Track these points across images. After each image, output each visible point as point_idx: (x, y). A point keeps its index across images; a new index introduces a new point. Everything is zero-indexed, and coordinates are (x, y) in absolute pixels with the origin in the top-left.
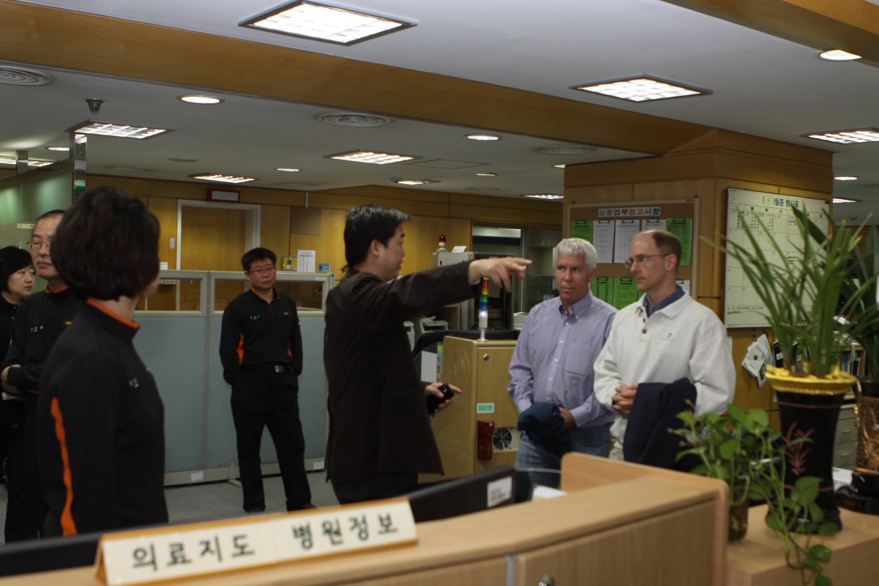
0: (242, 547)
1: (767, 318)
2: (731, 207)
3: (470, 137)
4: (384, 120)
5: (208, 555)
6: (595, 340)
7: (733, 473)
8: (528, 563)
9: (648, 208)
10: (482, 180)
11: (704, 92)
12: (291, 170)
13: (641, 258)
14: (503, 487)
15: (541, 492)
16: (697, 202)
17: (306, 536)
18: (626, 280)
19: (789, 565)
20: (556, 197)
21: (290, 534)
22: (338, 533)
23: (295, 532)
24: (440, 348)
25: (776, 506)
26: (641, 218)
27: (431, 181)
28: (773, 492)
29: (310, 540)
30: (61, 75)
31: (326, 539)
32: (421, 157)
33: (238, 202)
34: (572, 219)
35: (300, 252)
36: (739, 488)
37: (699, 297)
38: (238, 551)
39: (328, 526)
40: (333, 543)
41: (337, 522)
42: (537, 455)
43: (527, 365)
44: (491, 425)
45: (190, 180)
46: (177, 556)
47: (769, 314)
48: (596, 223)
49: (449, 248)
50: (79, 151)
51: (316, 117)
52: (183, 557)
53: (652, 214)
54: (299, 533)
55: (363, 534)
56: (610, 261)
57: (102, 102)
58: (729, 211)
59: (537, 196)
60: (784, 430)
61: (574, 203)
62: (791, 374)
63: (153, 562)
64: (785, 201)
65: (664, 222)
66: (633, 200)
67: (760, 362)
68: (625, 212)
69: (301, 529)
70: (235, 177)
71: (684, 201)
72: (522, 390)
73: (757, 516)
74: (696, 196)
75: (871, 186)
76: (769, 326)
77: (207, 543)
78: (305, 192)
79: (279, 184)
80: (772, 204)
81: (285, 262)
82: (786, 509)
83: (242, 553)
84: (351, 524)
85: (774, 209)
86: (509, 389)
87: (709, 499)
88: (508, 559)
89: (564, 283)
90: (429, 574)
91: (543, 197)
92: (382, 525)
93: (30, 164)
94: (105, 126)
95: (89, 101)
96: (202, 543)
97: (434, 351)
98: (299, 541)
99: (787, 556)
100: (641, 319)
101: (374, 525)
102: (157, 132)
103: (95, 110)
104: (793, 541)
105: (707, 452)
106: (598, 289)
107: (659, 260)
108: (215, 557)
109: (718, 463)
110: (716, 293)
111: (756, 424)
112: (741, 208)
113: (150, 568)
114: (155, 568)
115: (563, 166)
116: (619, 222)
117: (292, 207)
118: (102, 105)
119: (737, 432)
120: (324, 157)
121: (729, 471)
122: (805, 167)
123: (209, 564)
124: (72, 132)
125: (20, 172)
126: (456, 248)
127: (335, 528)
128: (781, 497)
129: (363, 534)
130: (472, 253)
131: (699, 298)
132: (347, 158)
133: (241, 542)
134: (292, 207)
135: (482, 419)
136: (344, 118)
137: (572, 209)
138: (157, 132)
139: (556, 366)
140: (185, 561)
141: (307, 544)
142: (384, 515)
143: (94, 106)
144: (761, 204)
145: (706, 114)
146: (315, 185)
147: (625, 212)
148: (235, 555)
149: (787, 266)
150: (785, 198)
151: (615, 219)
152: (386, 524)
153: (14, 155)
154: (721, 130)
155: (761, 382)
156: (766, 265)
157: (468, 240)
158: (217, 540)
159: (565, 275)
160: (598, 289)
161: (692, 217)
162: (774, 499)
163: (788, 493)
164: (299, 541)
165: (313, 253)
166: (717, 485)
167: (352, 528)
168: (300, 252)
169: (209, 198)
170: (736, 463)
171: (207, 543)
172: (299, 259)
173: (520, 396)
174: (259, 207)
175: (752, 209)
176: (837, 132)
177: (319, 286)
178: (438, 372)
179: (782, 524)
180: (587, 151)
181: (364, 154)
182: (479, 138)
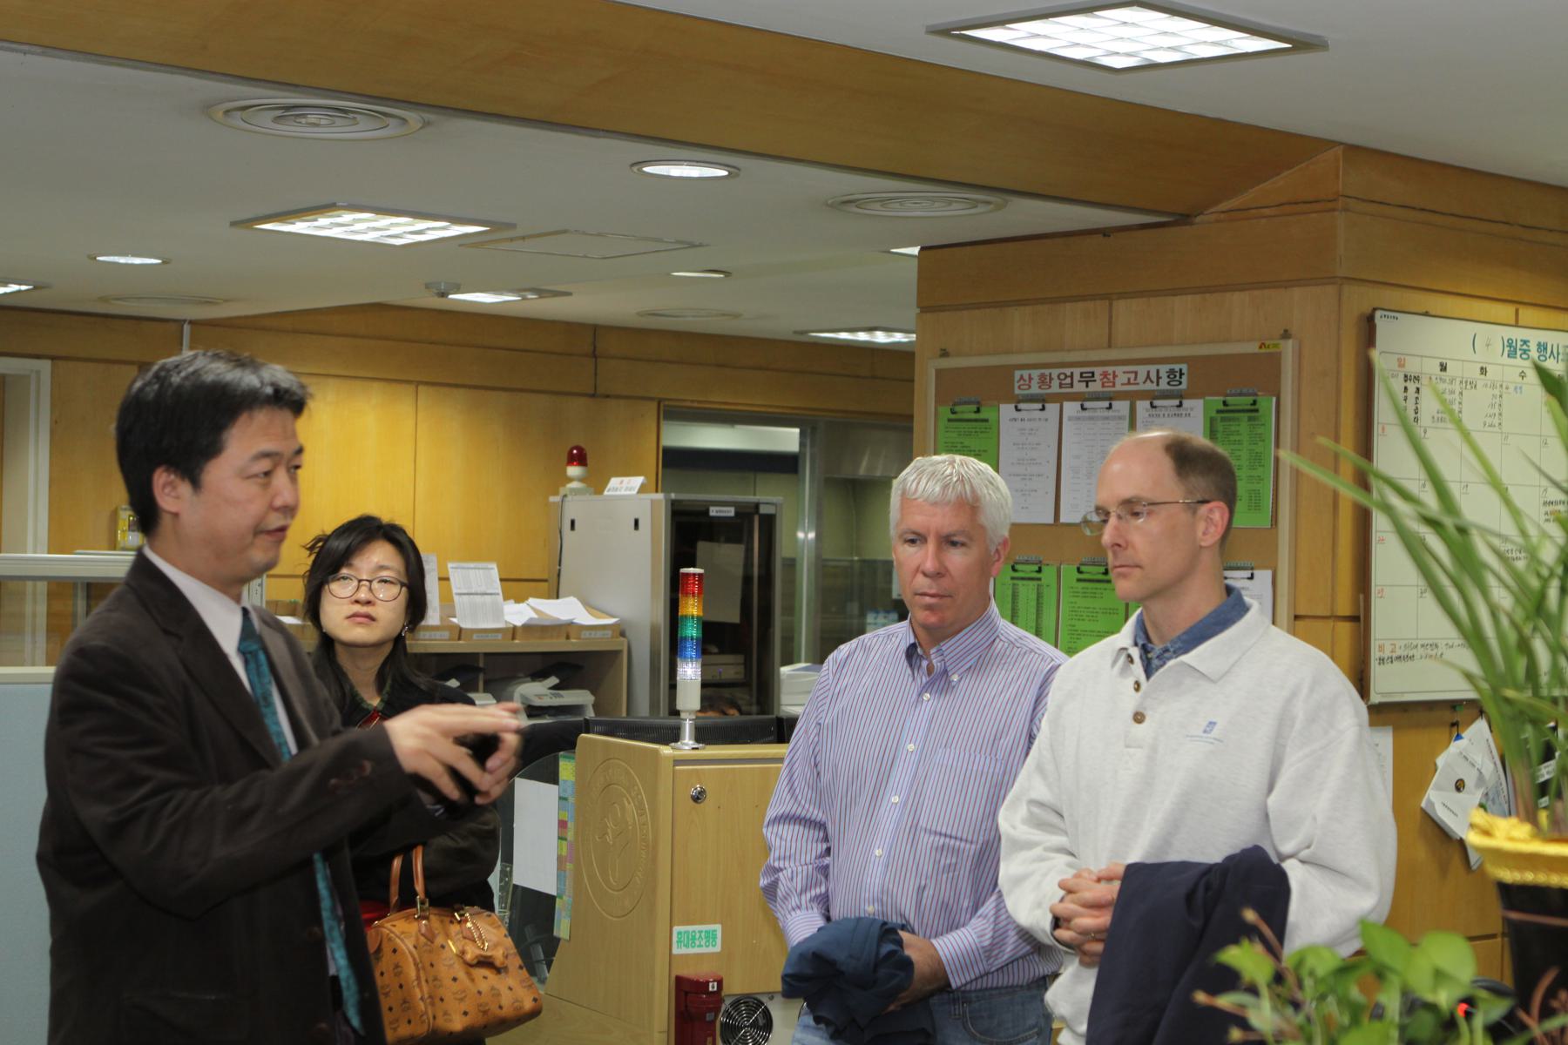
3: (647, 169)
4: (404, 121)
6: (1005, 742)
9: (1153, 369)
10: (685, 293)
11: (1301, 44)
12: (138, 261)
13: (1132, 507)
16: (1288, 348)
18: (1094, 571)
20: (898, 337)
26: (1133, 397)
27: (541, 293)
32: (512, 226)
34: (938, 402)
37: (1297, 617)
43: (817, 815)
44: (713, 987)
48: (1007, 410)
49: (596, 484)
51: (207, 108)
53: (1164, 385)
56: (1051, 521)
59: (844, 336)
61: (945, 354)
65: (1196, 406)
66: (1110, 346)
68: (1088, 379)
71: (1252, 348)
72: (799, 883)
74: (1286, 335)
78: (180, 323)
86: (763, 882)
89: (922, 582)
91: (862, 336)
97: (552, 778)
100: (1130, 682)
106: (1015, 596)
107: (1184, 517)
110: (1344, 608)
112: (1412, 367)
115: (915, 251)
116: (1071, 408)
120: (233, 224)
130: (660, 496)
131: (1298, 622)
132: (300, 227)
135: (689, 972)
136: (288, 112)
137: (940, 373)
146: (209, 302)
147: (1088, 379)
150: (1534, 337)
151: (1060, 398)
154: (1353, 151)
157: (651, 459)
160: (1015, 596)
173: (794, 901)
174: (45, 365)
175: (1443, 368)
180: (981, 209)
181: (347, 217)
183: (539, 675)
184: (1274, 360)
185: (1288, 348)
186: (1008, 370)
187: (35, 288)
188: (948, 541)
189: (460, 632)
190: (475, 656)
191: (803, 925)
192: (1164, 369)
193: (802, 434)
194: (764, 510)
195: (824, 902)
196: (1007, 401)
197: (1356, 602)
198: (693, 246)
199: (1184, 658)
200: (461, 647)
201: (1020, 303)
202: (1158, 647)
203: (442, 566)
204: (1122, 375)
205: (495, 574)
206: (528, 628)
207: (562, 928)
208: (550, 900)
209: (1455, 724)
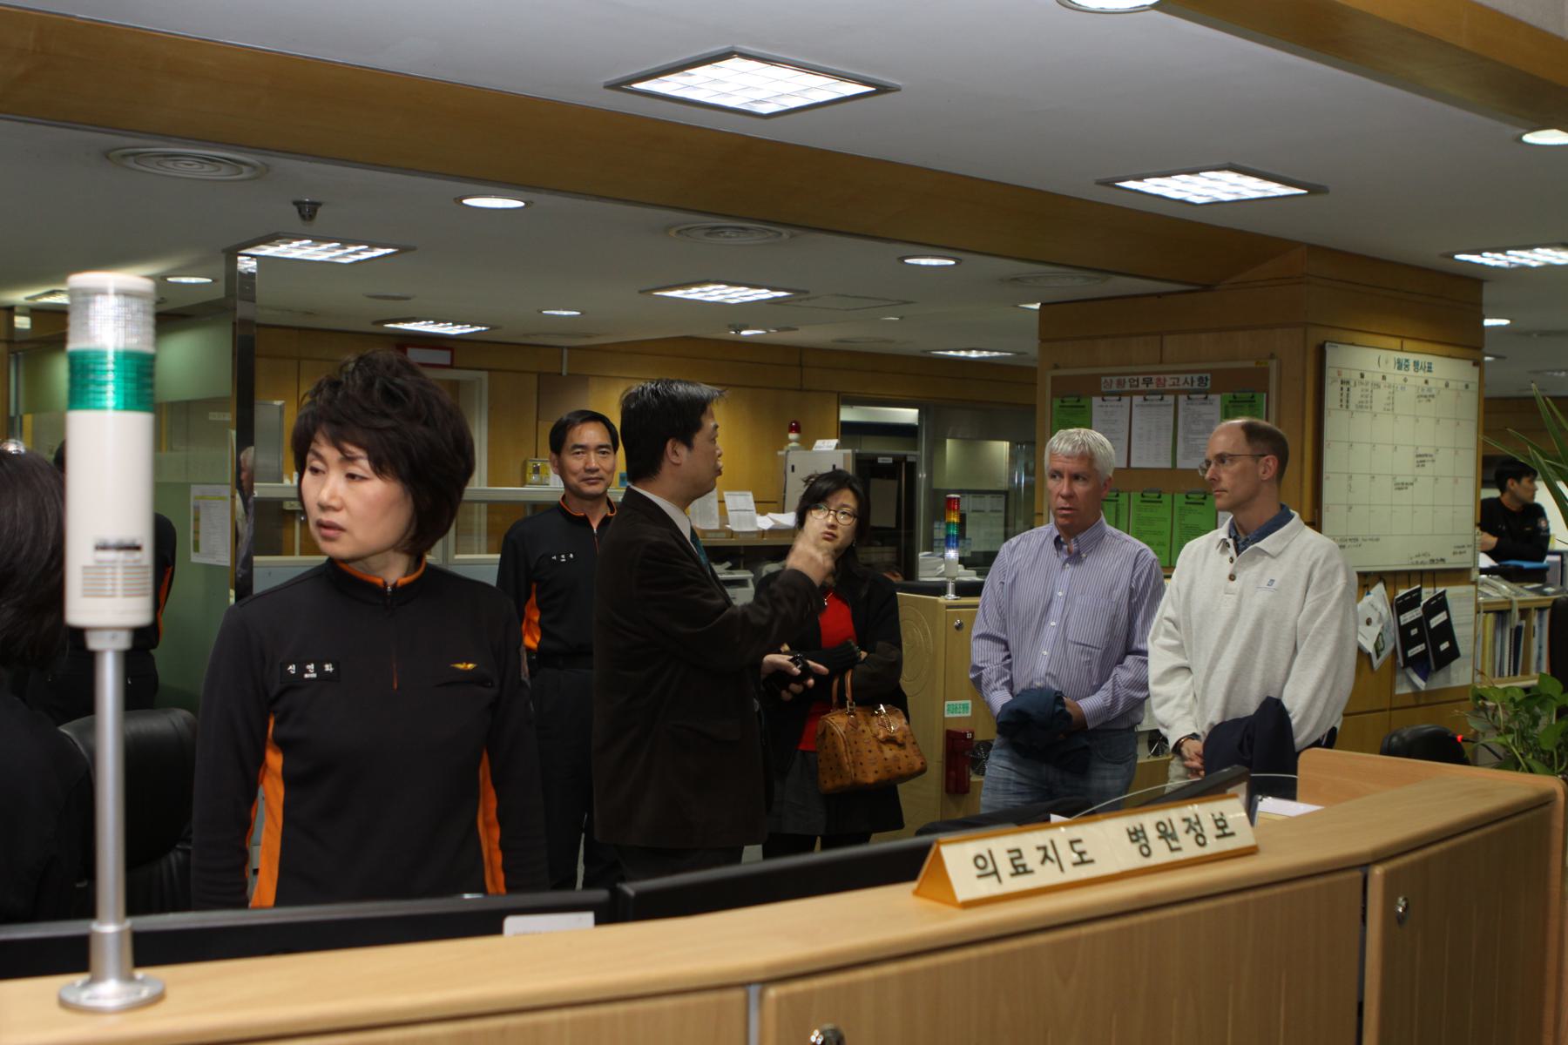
0: (1081, 854)
2: (1330, 373)
5: (1048, 863)
6: (1117, 593)
10: (885, 330)
11: (1314, 190)
13: (1221, 458)
16: (1273, 364)
20: (985, 354)
21: (1126, 836)
22: (1175, 839)
23: (1130, 834)
26: (1176, 393)
31: (1163, 842)
32: (806, 292)
33: (451, 366)
34: (1054, 395)
40: (1172, 850)
42: (1023, 780)
43: (1003, 636)
44: (969, 736)
48: (1096, 401)
49: (807, 444)
52: (1024, 866)
53: (1196, 386)
55: (1200, 839)
56: (1124, 465)
57: (318, 204)
58: (1328, 381)
59: (952, 353)
61: (1056, 367)
63: (996, 872)
65: (1216, 399)
66: (1161, 362)
67: (1375, 630)
68: (1148, 382)
69: (1136, 832)
71: (1252, 364)
72: (994, 676)
74: (1272, 356)
75: (1528, 334)
77: (1045, 848)
78: (561, 348)
79: (526, 335)
80: (1391, 369)
81: (530, 470)
83: (1083, 862)
84: (1186, 825)
85: (1396, 377)
86: (972, 676)
89: (1061, 502)
90: (1322, 881)
91: (962, 354)
94: (296, 244)
95: (299, 204)
98: (1136, 846)
100: (1227, 557)
101: (1210, 829)
103: (308, 218)
108: (1056, 865)
112: (1345, 376)
113: (994, 878)
114: (1000, 880)
115: (1037, 306)
116: (1137, 399)
117: (539, 374)
118: (320, 211)
122: (1440, 305)
123: (1046, 875)
124: (232, 254)
126: (819, 443)
127: (1170, 830)
129: (1200, 839)
130: (849, 451)
132: (678, 293)
134: (539, 374)
135: (953, 727)
136: (713, 231)
137: (1054, 379)
139: (1054, 632)
144: (1376, 368)
146: (588, 336)
147: (1148, 382)
150: (1412, 357)
151: (1131, 394)
154: (1313, 249)
155: (1376, 663)
157: (834, 428)
159: (1062, 486)
164: (1136, 846)
171: (1045, 848)
173: (992, 686)
174: (484, 375)
176: (1503, 250)
182: (924, 262)
184: (1265, 372)
185: (1273, 364)
186: (1096, 379)
187: (492, 328)
188: (1075, 477)
189: (732, 533)
191: (1000, 698)
192: (1196, 377)
193: (920, 413)
194: (909, 459)
195: (1010, 685)
196: (1097, 395)
197: (1313, 514)
198: (906, 302)
199: (1258, 545)
200: (733, 542)
201: (1105, 337)
202: (1242, 537)
203: (721, 495)
204: (1169, 381)
205: (750, 497)
206: (771, 531)
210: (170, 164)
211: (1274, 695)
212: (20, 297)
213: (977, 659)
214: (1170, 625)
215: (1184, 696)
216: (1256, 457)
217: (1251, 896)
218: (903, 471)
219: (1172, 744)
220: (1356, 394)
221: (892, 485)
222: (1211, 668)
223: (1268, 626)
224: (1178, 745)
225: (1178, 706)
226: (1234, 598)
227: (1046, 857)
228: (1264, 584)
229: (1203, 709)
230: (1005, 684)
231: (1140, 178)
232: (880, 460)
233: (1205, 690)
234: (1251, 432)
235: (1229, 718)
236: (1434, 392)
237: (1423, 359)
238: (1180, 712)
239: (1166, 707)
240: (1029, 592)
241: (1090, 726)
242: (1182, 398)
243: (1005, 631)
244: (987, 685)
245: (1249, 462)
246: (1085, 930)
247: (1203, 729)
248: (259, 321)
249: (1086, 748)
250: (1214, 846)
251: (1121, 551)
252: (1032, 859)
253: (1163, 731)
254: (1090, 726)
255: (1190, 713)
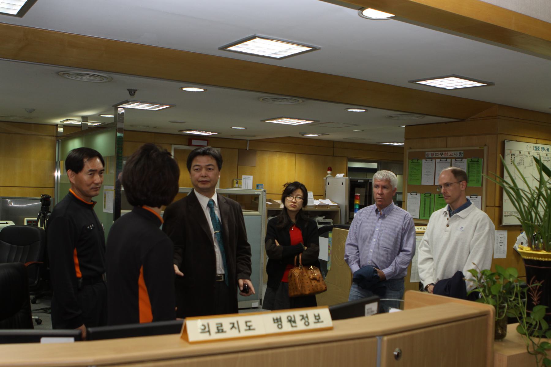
0: (249, 326)
1: (518, 218)
2: (507, 152)
5: (234, 329)
7: (498, 303)
8: (388, 341)
11: (489, 84)
14: (374, 306)
15: (393, 310)
16: (486, 148)
17: (280, 323)
19: (529, 352)
20: (399, 144)
21: (272, 321)
22: (294, 322)
23: (274, 320)
24: (330, 235)
25: (522, 322)
26: (451, 158)
27: (323, 134)
28: (521, 313)
29: (281, 325)
30: (116, 76)
31: (289, 324)
32: (319, 121)
34: (409, 159)
35: (244, 177)
36: (501, 310)
38: (248, 328)
39: (289, 318)
40: (292, 326)
41: (294, 316)
45: (180, 133)
46: (220, 330)
47: (519, 217)
48: (424, 161)
49: (334, 175)
50: (119, 118)
52: (222, 330)
53: (458, 156)
54: (276, 321)
56: (433, 184)
57: (136, 90)
60: (528, 282)
61: (411, 148)
62: (532, 249)
63: (209, 331)
64: (540, 148)
65: (465, 160)
68: (442, 154)
69: (277, 319)
70: (206, 132)
71: (478, 148)
73: (512, 329)
74: (485, 145)
76: (520, 224)
77: (233, 324)
78: (247, 140)
81: (235, 182)
82: (527, 323)
83: (250, 329)
84: (301, 318)
87: (484, 315)
88: (378, 338)
91: (392, 144)
92: (316, 319)
93: (89, 124)
94: (136, 104)
95: (130, 90)
96: (231, 323)
97: (327, 237)
98: (276, 325)
99: (528, 347)
101: (312, 319)
102: (165, 107)
103: (133, 95)
104: (531, 340)
105: (484, 291)
106: (425, 201)
108: (237, 330)
109: (490, 297)
110: (497, 204)
111: (511, 276)
112: (513, 152)
113: (208, 334)
114: (210, 334)
116: (438, 160)
117: (239, 150)
118: (136, 93)
119: (501, 281)
121: (496, 301)
123: (234, 334)
124: (116, 107)
125: (83, 129)
126: (338, 175)
127: (293, 319)
128: (525, 316)
132: (275, 122)
133: (249, 324)
134: (239, 150)
137: (409, 152)
138: (165, 107)
140: (223, 331)
141: (280, 326)
142: (317, 314)
143: (132, 92)
145: (491, 96)
147: (442, 154)
148: (246, 330)
149: (530, 191)
150: (541, 146)
151: (435, 158)
152: (318, 318)
153: (80, 119)
154: (501, 106)
156: (518, 190)
157: (345, 170)
158: (237, 322)
160: (425, 201)
161: (483, 158)
162: (521, 318)
163: (528, 315)
164: (276, 325)
165: (251, 177)
166: (489, 308)
167: (301, 320)
168: (244, 177)
169: (190, 144)
170: (500, 297)
172: (243, 181)
175: (520, 153)
177: (256, 197)
178: (329, 249)
179: (525, 331)
181: (285, 119)
182: (354, 110)
183: (321, 216)
184: (482, 151)
190: (308, 211)
197: (500, 203)
204: (449, 154)
206: (319, 205)
207: (329, 268)
208: (326, 262)
209: (521, 230)
210: (80, 77)
211: (460, 270)
212: (58, 121)
213: (347, 253)
214: (426, 243)
215: (430, 269)
216: (459, 182)
217: (322, 346)
218: (368, 185)
219: (424, 286)
220: (517, 160)
221: (363, 190)
222: (439, 259)
223: (460, 244)
224: (427, 287)
225: (427, 273)
226: (448, 233)
227: (233, 327)
228: (459, 228)
229: (436, 274)
230: (357, 262)
231: (424, 80)
232: (359, 181)
233: (437, 267)
234: (455, 173)
235: (445, 278)
236: (550, 159)
237: (545, 146)
238: (428, 275)
239: (423, 273)
240: (366, 228)
241: (387, 279)
242: (453, 160)
243: (357, 242)
244: (351, 262)
245: (458, 185)
246: (240, 355)
247: (435, 282)
248: (124, 129)
249: (385, 287)
250: (312, 326)
251: (398, 217)
252: (226, 326)
253: (422, 282)
254: (387, 279)
255: (431, 275)
